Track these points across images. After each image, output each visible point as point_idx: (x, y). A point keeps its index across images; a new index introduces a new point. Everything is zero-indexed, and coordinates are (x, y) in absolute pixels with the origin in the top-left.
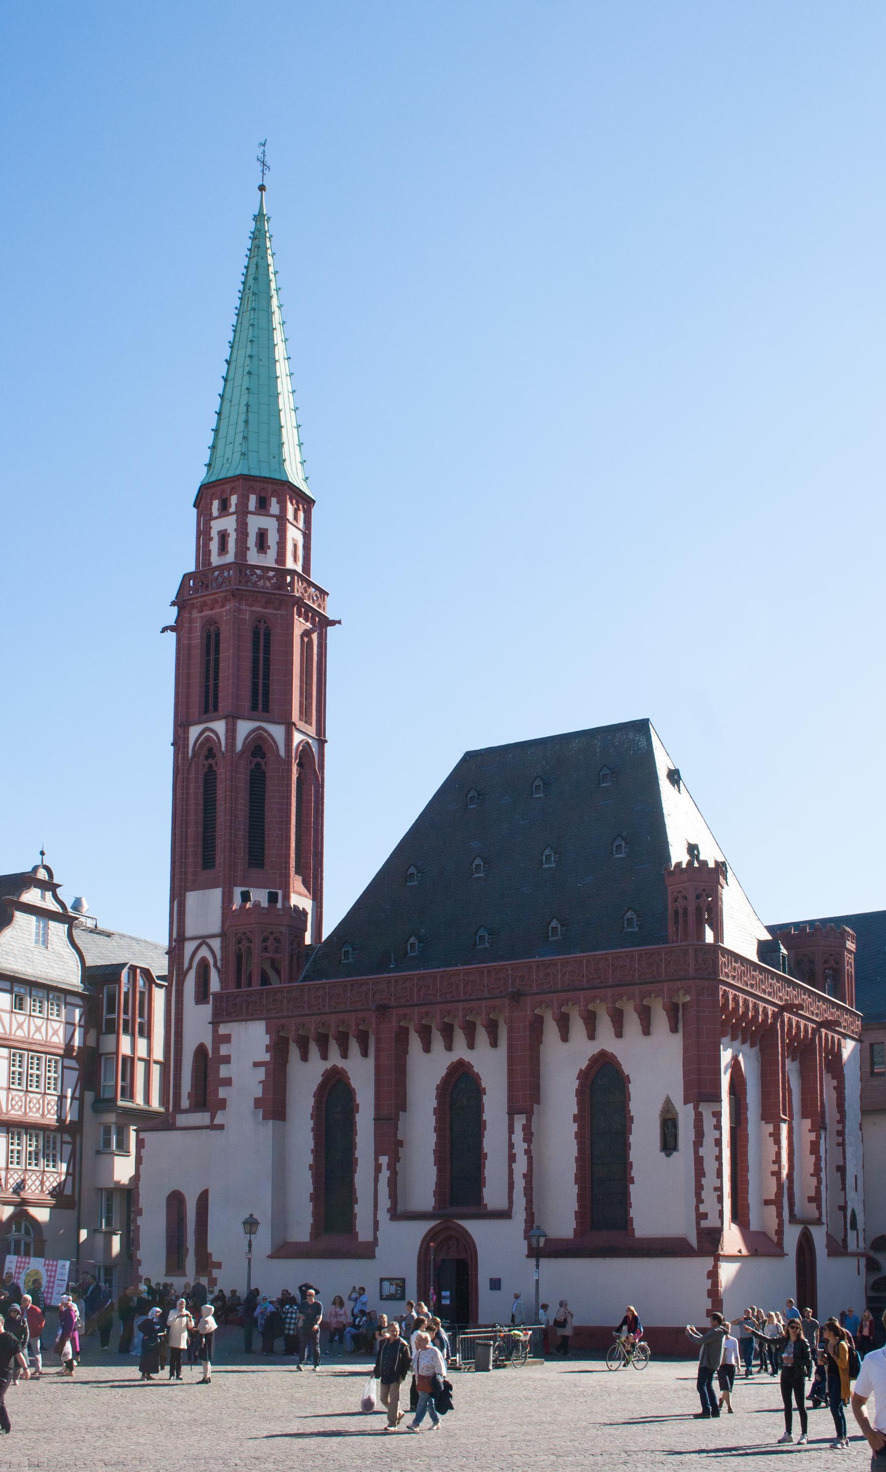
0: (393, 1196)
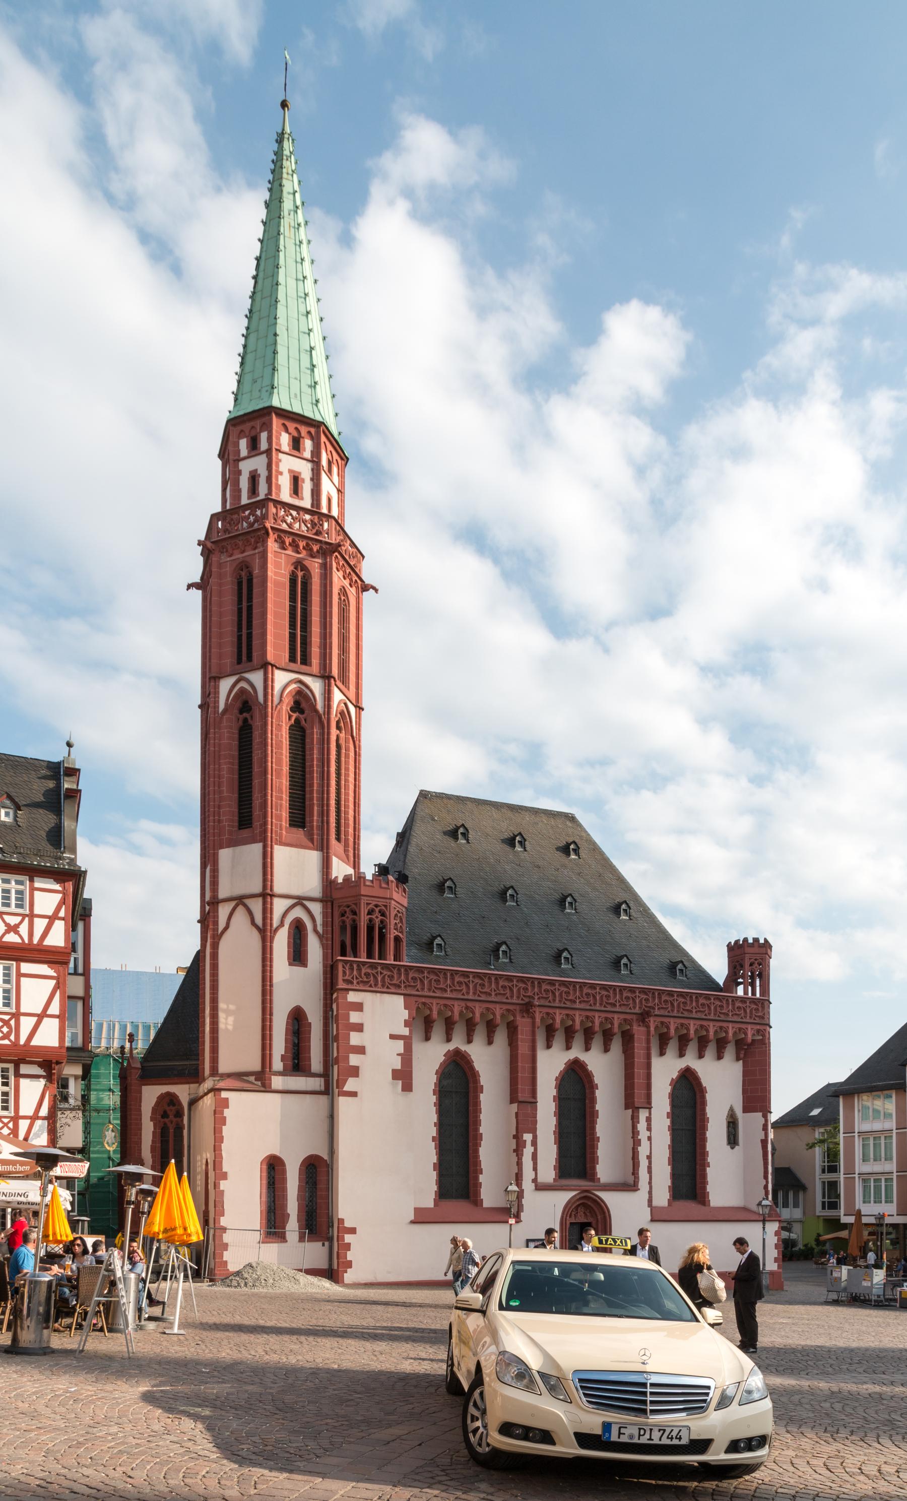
0: (535, 1169)
